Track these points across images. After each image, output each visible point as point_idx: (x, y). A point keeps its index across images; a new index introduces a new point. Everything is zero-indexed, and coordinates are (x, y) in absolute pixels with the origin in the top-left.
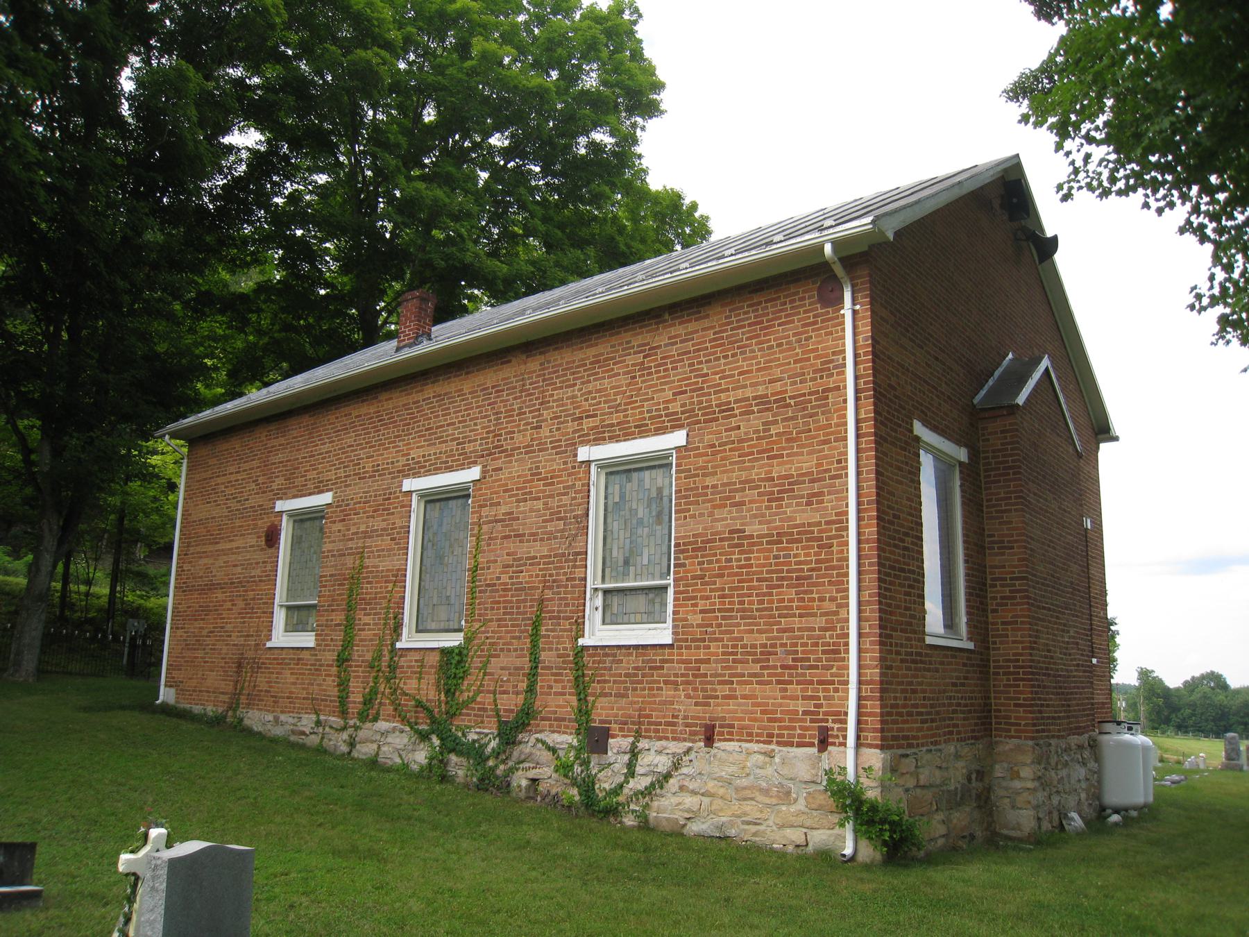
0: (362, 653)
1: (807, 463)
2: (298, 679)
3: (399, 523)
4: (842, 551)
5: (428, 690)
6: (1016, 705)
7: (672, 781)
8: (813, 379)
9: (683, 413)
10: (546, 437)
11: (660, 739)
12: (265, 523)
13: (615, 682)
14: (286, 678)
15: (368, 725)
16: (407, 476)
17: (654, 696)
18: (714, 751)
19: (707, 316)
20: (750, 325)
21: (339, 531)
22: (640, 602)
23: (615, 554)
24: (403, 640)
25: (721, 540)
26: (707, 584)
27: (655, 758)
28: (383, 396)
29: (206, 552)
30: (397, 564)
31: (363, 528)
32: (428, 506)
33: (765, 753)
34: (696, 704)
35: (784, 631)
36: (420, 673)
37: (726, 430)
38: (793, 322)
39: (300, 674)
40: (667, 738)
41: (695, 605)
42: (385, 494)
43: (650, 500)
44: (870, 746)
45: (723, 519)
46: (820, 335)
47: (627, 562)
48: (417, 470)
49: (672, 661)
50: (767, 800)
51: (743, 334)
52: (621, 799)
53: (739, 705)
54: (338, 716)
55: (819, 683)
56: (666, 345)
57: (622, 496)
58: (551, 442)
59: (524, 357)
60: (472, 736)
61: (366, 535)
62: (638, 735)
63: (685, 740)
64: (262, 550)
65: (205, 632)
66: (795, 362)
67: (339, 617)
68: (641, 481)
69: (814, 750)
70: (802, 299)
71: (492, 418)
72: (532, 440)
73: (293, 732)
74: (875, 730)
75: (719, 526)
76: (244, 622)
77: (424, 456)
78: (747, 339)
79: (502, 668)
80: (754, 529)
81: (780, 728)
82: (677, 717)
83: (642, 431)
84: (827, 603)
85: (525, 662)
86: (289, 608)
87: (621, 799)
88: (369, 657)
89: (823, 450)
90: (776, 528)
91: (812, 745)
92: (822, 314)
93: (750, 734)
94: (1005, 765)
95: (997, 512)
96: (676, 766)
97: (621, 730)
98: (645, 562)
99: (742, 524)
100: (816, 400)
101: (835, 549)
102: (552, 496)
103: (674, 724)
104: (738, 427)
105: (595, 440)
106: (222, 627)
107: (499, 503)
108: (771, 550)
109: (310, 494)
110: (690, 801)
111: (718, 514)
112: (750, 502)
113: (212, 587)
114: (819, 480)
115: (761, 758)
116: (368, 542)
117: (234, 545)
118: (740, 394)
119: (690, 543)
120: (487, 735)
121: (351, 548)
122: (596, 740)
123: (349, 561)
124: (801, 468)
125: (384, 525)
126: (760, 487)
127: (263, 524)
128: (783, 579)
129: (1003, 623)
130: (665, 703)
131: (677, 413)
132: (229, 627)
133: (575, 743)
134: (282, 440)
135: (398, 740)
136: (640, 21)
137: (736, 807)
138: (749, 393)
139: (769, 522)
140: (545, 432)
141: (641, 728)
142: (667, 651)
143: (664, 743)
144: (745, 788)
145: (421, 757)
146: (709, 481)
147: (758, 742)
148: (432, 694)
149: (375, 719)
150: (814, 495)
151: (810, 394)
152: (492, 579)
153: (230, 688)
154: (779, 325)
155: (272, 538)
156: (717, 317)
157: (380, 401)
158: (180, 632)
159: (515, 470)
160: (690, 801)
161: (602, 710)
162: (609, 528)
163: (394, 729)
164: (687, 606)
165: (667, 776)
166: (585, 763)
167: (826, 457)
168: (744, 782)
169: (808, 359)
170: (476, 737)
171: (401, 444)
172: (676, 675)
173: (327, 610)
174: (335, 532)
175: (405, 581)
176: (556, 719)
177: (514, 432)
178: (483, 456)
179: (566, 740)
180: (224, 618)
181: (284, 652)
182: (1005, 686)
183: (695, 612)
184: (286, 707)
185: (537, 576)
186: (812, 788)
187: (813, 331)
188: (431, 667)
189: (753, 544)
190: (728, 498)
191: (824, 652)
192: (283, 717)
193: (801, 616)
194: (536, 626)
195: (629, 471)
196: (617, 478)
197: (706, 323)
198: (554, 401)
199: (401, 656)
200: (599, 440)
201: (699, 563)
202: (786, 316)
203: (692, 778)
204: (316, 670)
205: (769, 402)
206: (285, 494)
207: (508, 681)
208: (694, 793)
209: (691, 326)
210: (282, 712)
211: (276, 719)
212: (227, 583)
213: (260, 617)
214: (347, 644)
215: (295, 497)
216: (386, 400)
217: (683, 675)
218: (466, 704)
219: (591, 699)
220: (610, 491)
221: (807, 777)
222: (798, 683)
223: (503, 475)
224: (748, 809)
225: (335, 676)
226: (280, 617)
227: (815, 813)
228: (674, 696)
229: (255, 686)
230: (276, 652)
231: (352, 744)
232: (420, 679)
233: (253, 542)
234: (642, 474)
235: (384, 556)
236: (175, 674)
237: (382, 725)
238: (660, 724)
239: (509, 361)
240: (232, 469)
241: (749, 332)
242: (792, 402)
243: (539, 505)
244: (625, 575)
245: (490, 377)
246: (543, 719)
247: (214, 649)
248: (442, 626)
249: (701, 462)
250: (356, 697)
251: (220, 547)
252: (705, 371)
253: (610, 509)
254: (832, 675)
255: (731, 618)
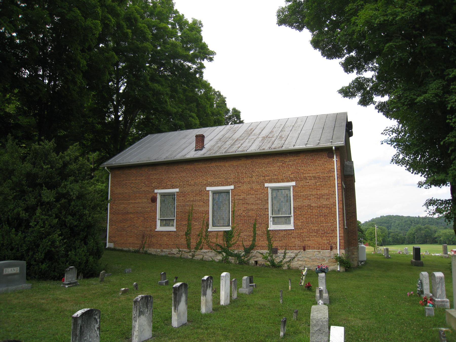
0: (194, 232)
1: (326, 191)
2: (169, 239)
3: (205, 198)
4: (334, 210)
5: (220, 241)
6: (353, 240)
7: (295, 259)
8: (326, 174)
9: (294, 178)
10: (254, 180)
11: (292, 250)
12: (150, 195)
13: (278, 238)
14: (164, 239)
15: (199, 251)
16: (208, 186)
17: (290, 241)
18: (306, 252)
19: (299, 156)
20: (311, 160)
21: (182, 199)
22: (283, 219)
23: (275, 208)
24: (210, 228)
25: (305, 207)
26: (302, 216)
27: (290, 254)
28: (196, 164)
29: (124, 203)
30: (206, 209)
31: (192, 199)
32: (214, 194)
33: (318, 252)
34: (301, 242)
35: (322, 226)
36: (217, 237)
37: (305, 183)
38: (321, 160)
39: (170, 238)
40: (293, 250)
41: (300, 221)
42: (199, 190)
43: (284, 197)
44: (342, 249)
45: (305, 202)
46: (328, 164)
47: (279, 211)
48: (211, 185)
49: (294, 233)
50: (319, 261)
51: (309, 161)
52: (282, 263)
53: (312, 242)
54: (187, 249)
55: (330, 237)
56: (288, 162)
57: (277, 195)
58: (256, 181)
59: (246, 159)
60: (236, 252)
61: (193, 201)
62: (286, 249)
63: (298, 250)
64: (150, 203)
65: (126, 226)
66: (322, 169)
67: (185, 223)
68: (282, 192)
69: (329, 250)
70: (324, 156)
71: (236, 173)
72: (250, 180)
73: (169, 254)
74: (343, 246)
75: (305, 204)
76: (144, 224)
77: (213, 181)
78: (310, 163)
79: (244, 235)
80: (314, 205)
81: (321, 246)
82: (296, 245)
83: (283, 181)
84: (331, 221)
85: (252, 234)
86: (161, 220)
87: (282, 263)
88: (198, 233)
89: (329, 189)
90: (319, 205)
91: (329, 249)
92: (328, 160)
93: (314, 248)
94: (351, 252)
95: (349, 198)
96: (296, 255)
97: (281, 248)
98: (284, 210)
99: (310, 204)
100: (327, 178)
101: (333, 210)
102: (257, 194)
103: (295, 247)
104: (309, 182)
105: (269, 182)
106: (134, 225)
107: (240, 195)
108: (318, 209)
109: (169, 189)
110: (300, 263)
111: (304, 201)
112: (312, 199)
113: (128, 213)
114: (329, 195)
115: (317, 252)
116: (194, 203)
117: (137, 201)
118: (309, 175)
119: (297, 207)
120: (241, 251)
121: (188, 204)
122: (274, 251)
123: (187, 208)
124: (324, 192)
125: (200, 199)
126: (315, 196)
127: (150, 196)
128: (321, 215)
129: (350, 222)
130: (292, 242)
131: (292, 178)
132: (136, 225)
133: (268, 252)
134: (155, 172)
135: (210, 254)
136: (410, 173)
137: (312, 263)
138: (311, 175)
139: (317, 203)
140: (254, 178)
141: (286, 247)
142: (292, 231)
143: (293, 251)
144: (314, 259)
145: (219, 257)
146: (302, 194)
147: (316, 249)
148: (221, 242)
149: (202, 249)
150: (328, 198)
151: (326, 177)
152: (239, 214)
153: (140, 242)
154: (318, 161)
155: (154, 200)
156: (302, 157)
157: (195, 165)
158: (113, 227)
159: (245, 187)
160: (300, 263)
161: (275, 244)
162: (273, 202)
163: (209, 251)
164: (297, 221)
165: (294, 258)
166: (272, 256)
167: (330, 190)
168: (314, 258)
169: (325, 169)
170: (237, 252)
171: (204, 177)
172: (295, 236)
173: (179, 221)
174: (181, 199)
175: (209, 214)
176: (262, 247)
177: (244, 178)
178: (234, 183)
179: (265, 251)
180: (135, 223)
181: (163, 232)
182: (350, 235)
183: (299, 222)
184: (165, 247)
185: (254, 213)
186: (329, 258)
187: (326, 163)
188: (221, 235)
189: (314, 208)
190: (307, 197)
191: (331, 231)
192: (164, 250)
193: (325, 223)
194: (255, 225)
195: (278, 189)
196: (275, 191)
197: (299, 158)
198: (256, 171)
199: (210, 233)
200: (271, 182)
201: (300, 212)
202: (320, 159)
203: (301, 258)
204: (177, 237)
205: (316, 178)
206: (159, 188)
207: (247, 238)
208: (301, 261)
209: (295, 158)
210: (163, 249)
211: (162, 251)
212: (135, 212)
213: (151, 222)
214: (189, 229)
215: (162, 189)
216: (197, 165)
217: (297, 236)
218: (233, 244)
219: (272, 242)
220: (273, 194)
221: (329, 256)
222: (325, 237)
223: (241, 188)
224: (315, 263)
225: (185, 238)
226: (158, 223)
227: (330, 263)
228: (295, 241)
229: (151, 242)
230: (159, 232)
231: (193, 256)
232: (217, 238)
233: (146, 201)
234: (281, 190)
235: (201, 207)
236: (113, 239)
237: (204, 250)
238: (292, 247)
239: (241, 160)
240: (133, 179)
241: (310, 161)
242: (322, 178)
243: (254, 196)
244: (279, 214)
245: (235, 163)
246: (258, 247)
247: (131, 231)
248: (221, 225)
249: (299, 189)
250: (193, 243)
251: (130, 201)
252: (299, 169)
253: (273, 198)
254: (333, 235)
255: (309, 223)
